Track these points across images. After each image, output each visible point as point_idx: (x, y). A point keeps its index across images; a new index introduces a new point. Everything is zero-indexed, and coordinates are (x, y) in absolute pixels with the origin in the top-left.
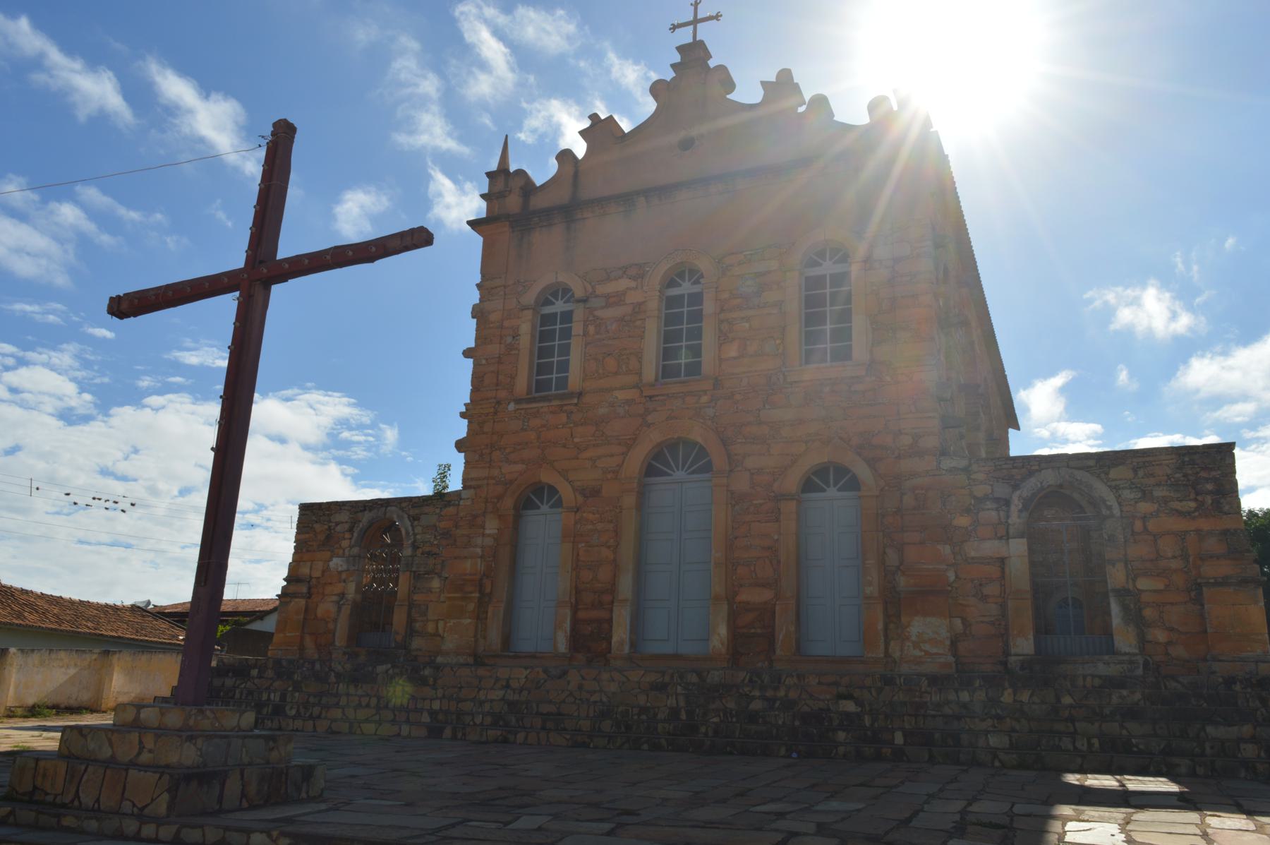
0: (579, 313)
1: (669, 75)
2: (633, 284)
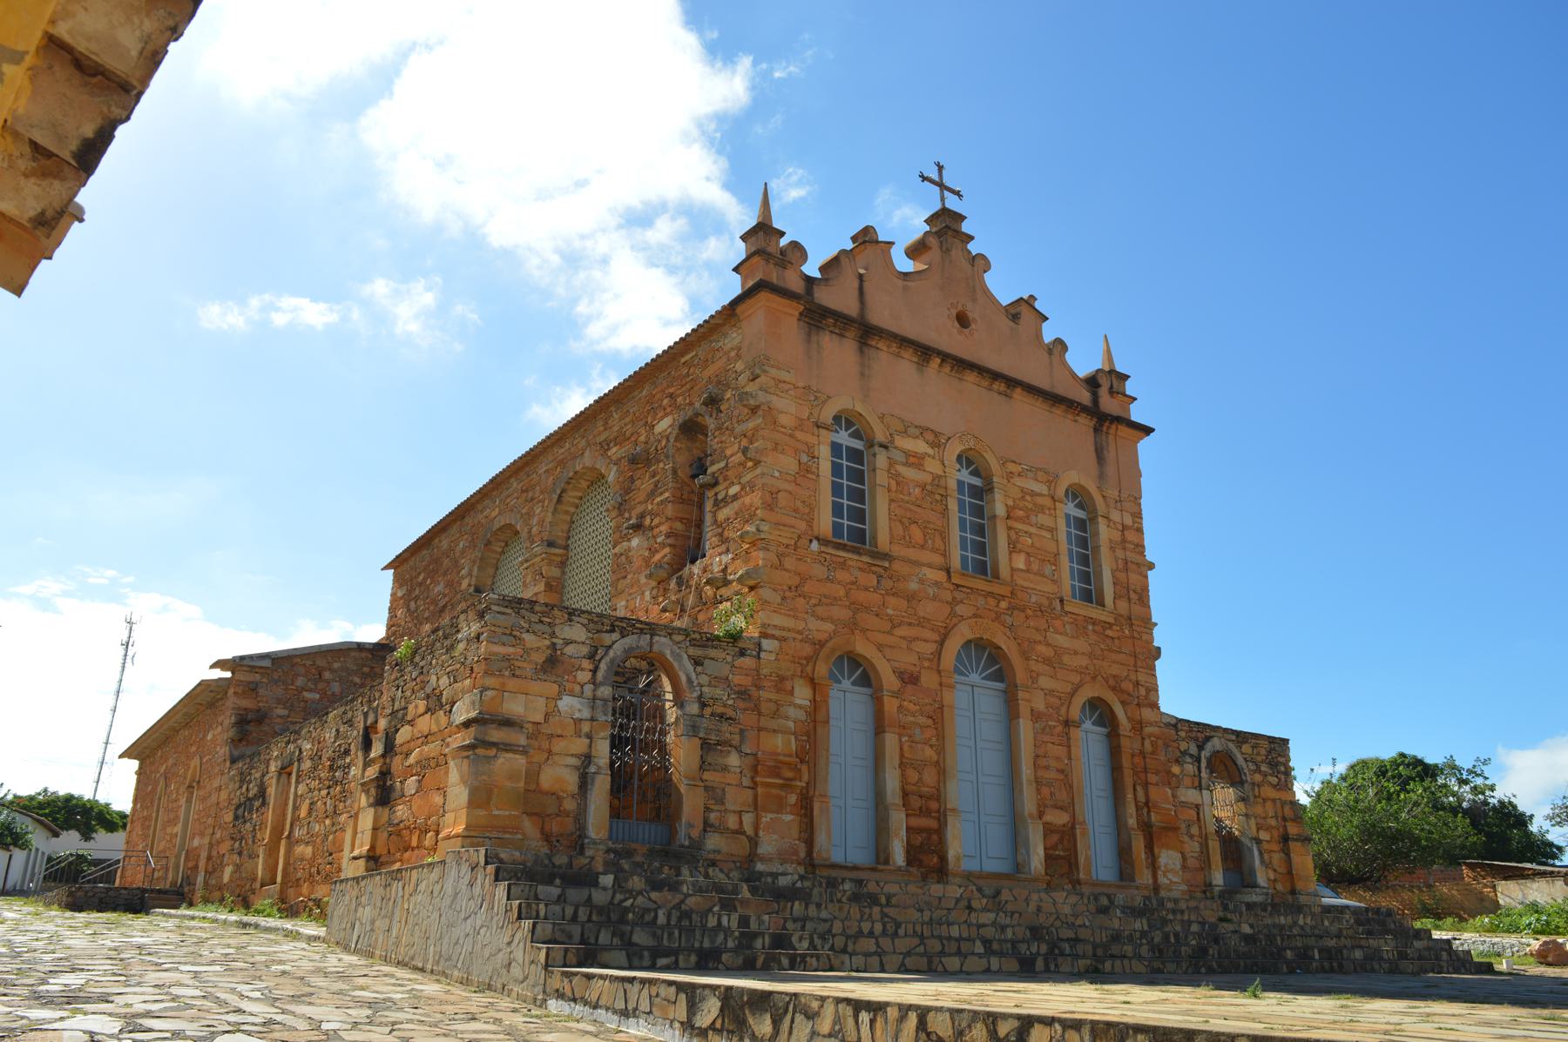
2: (930, 451)
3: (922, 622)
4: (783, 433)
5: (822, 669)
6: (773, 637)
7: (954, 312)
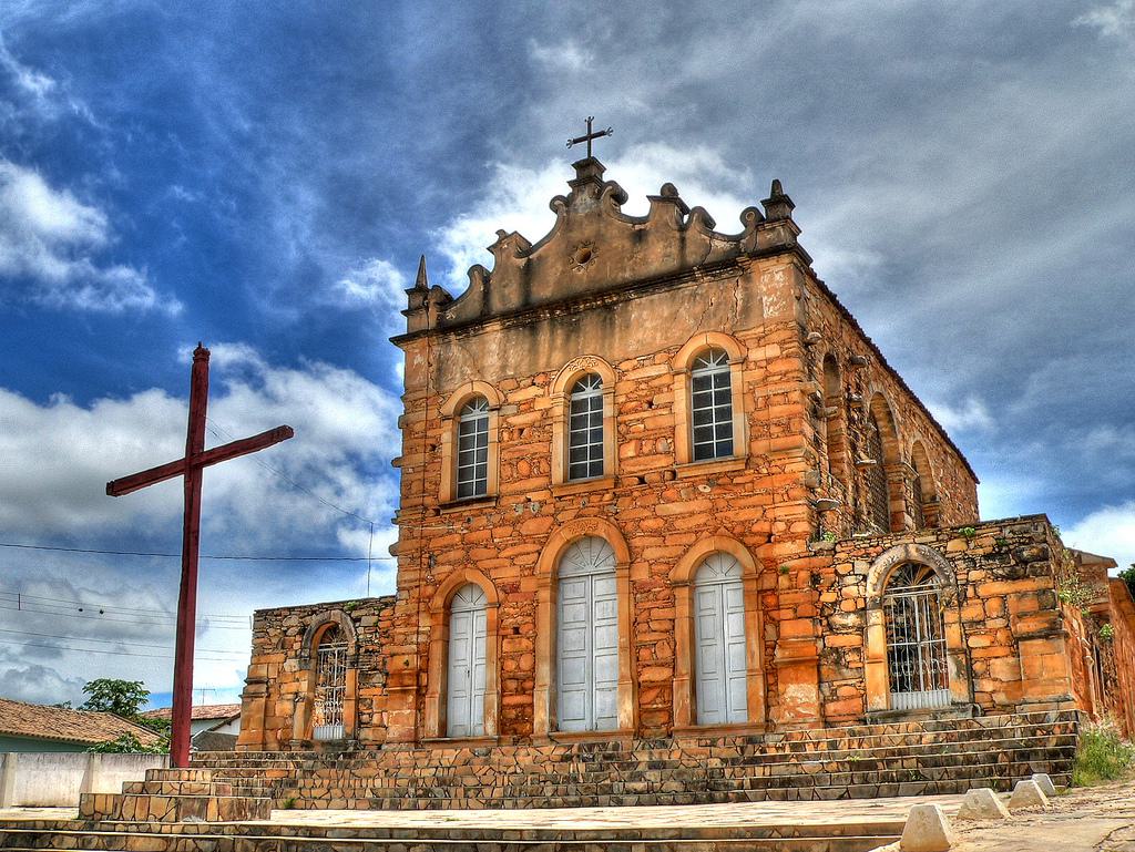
0: (494, 419)
1: (566, 191)
2: (541, 392)
3: (524, 539)
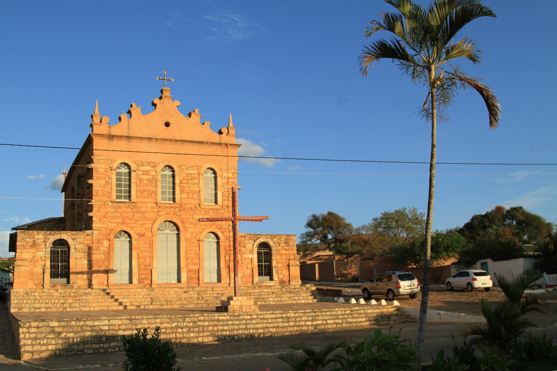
2: (152, 169)
3: (147, 219)
4: (101, 174)
5: (112, 236)
6: (96, 230)
7: (164, 123)
